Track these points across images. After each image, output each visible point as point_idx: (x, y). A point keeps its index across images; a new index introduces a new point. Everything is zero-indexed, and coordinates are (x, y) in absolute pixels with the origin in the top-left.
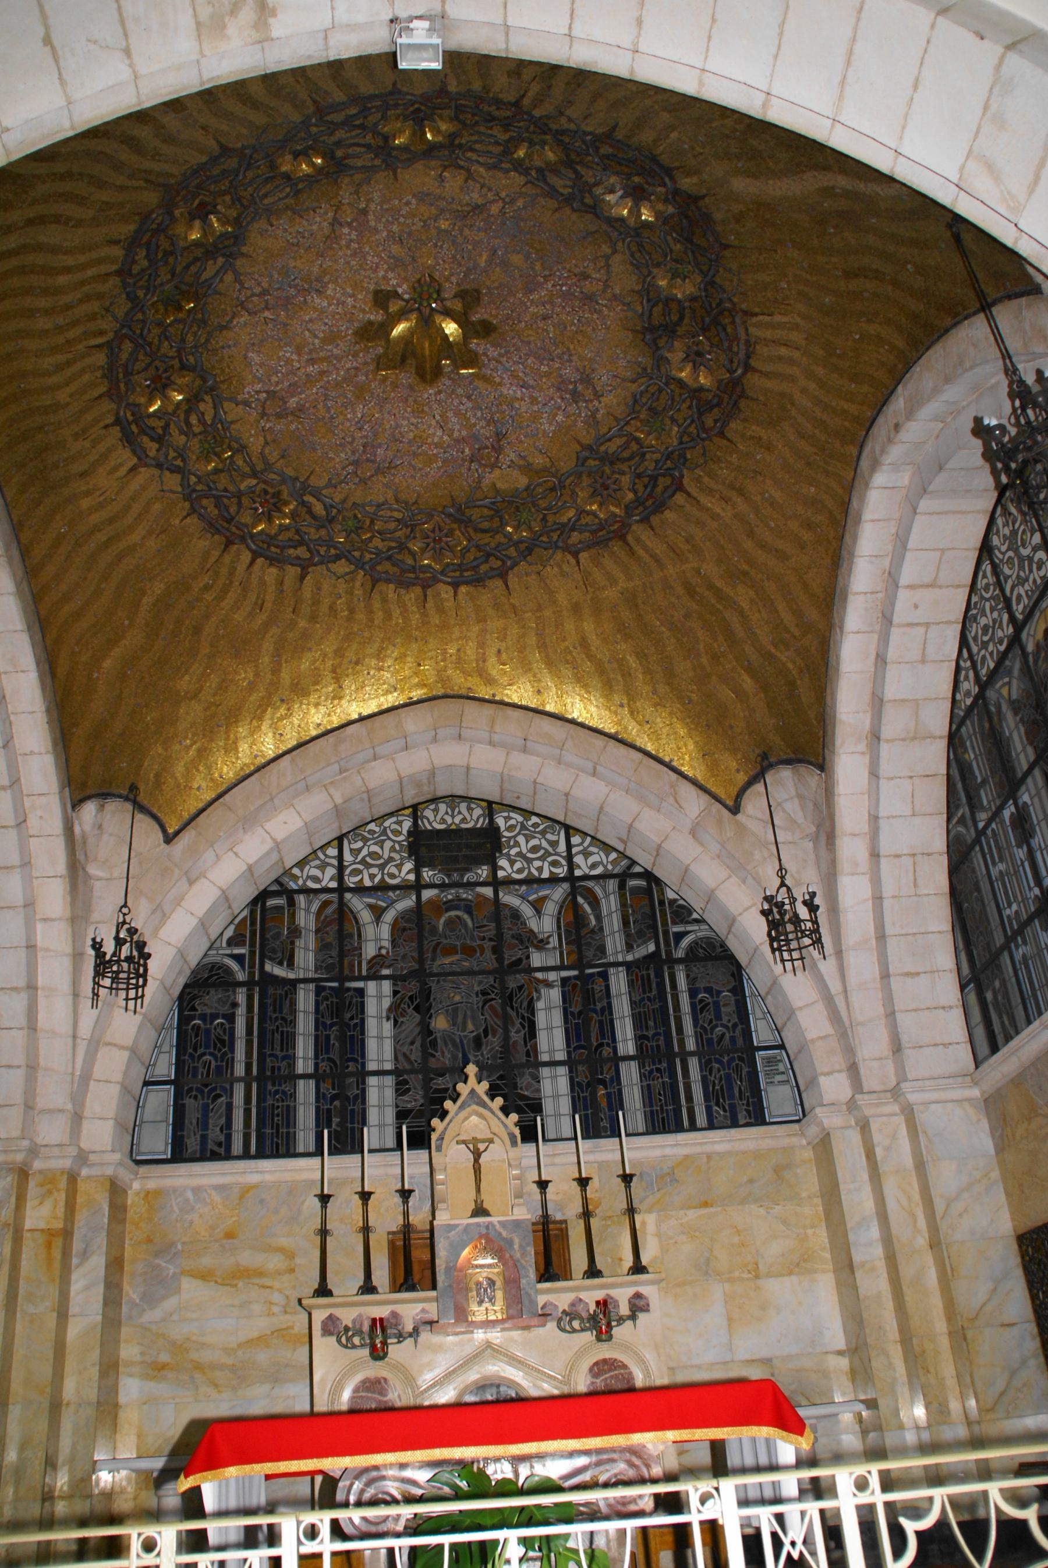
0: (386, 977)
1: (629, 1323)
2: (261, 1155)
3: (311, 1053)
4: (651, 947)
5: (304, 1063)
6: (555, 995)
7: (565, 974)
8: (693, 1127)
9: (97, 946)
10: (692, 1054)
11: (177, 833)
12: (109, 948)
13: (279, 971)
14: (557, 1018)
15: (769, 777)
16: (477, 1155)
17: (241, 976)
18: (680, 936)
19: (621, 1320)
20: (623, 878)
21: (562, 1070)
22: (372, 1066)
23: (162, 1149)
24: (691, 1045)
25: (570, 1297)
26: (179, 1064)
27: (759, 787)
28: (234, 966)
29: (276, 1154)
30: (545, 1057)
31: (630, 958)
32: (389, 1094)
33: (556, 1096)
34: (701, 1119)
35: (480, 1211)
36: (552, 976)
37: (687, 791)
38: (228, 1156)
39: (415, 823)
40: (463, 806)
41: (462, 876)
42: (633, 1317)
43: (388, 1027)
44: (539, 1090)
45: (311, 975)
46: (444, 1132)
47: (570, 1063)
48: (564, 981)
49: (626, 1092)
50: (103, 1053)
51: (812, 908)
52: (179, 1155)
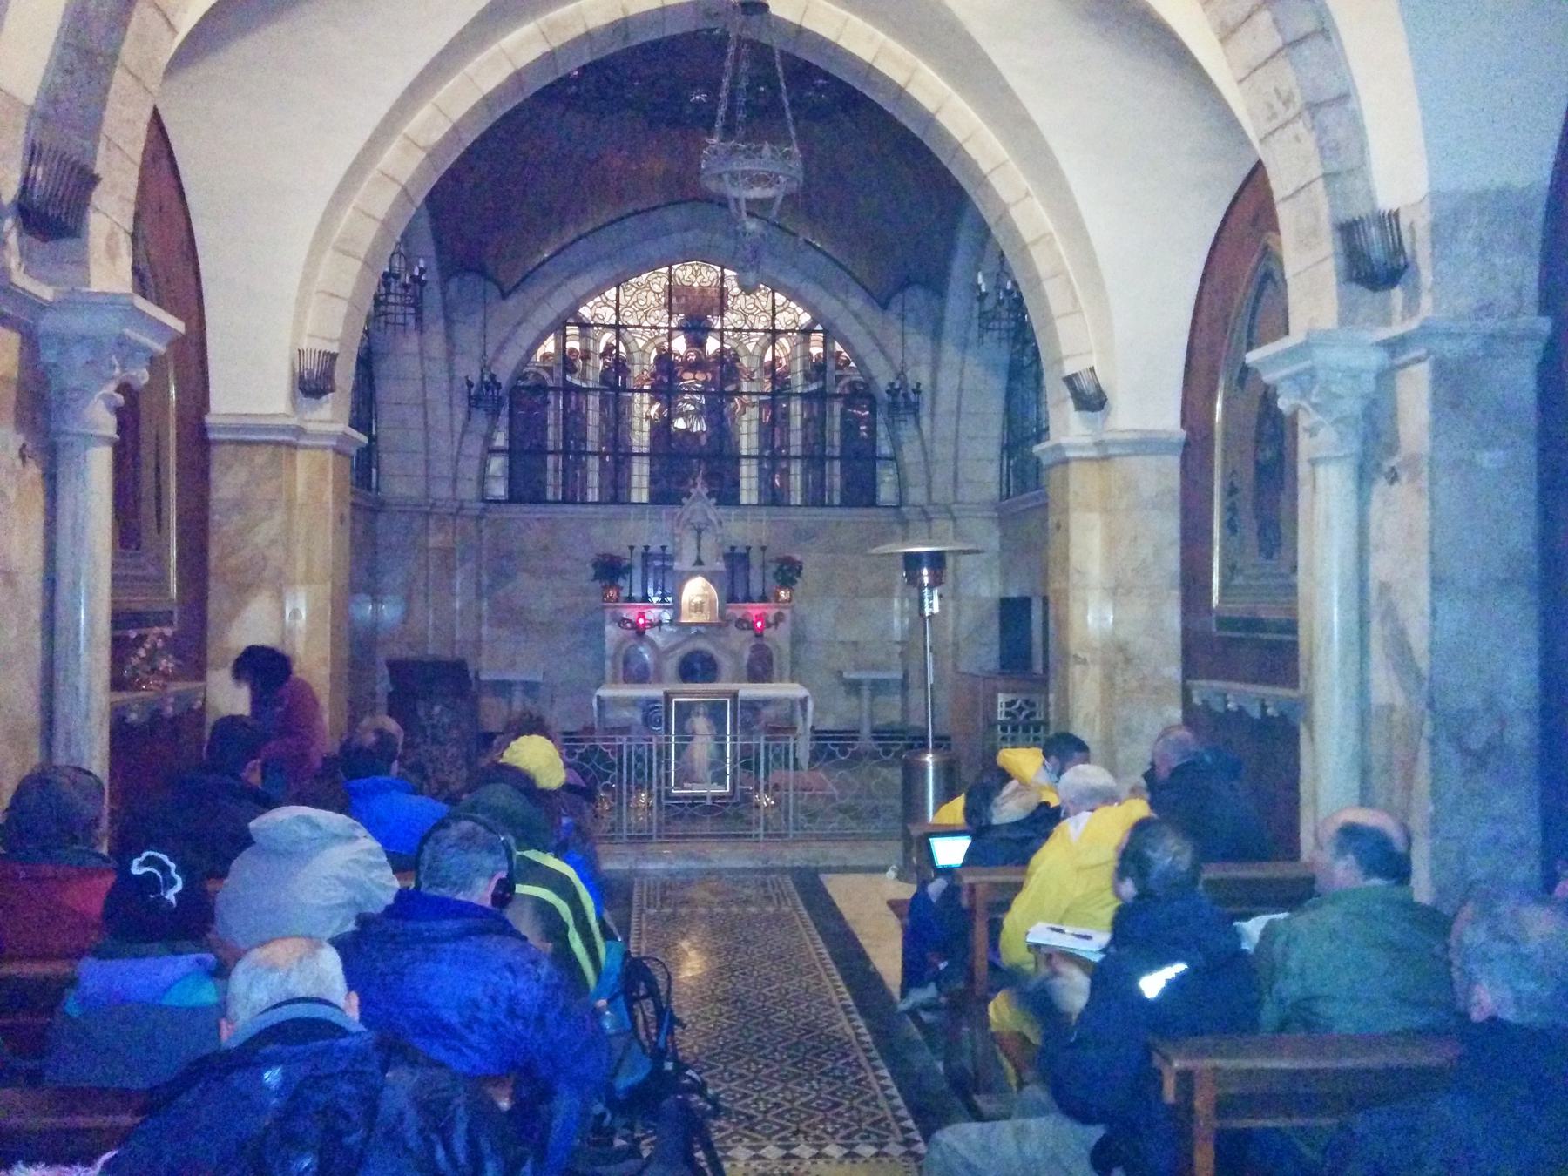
0: (646, 391)
1: (773, 628)
2: (565, 501)
3: (596, 438)
4: (821, 383)
5: (592, 445)
6: (754, 412)
7: (762, 398)
8: (831, 505)
9: (470, 385)
10: (836, 458)
11: (510, 293)
12: (475, 379)
13: (577, 382)
14: (754, 426)
15: (909, 291)
16: (699, 531)
17: (550, 383)
18: (839, 378)
19: (769, 625)
20: (807, 332)
21: (754, 462)
22: (635, 450)
23: (502, 493)
24: (837, 453)
25: (743, 611)
26: (511, 439)
27: (900, 296)
28: (545, 374)
29: (573, 502)
30: (744, 453)
31: (805, 391)
32: (646, 469)
33: (749, 477)
34: (837, 501)
35: (699, 562)
36: (754, 399)
37: (854, 287)
38: (546, 502)
39: (670, 280)
40: (704, 269)
41: (700, 321)
42: (776, 624)
43: (646, 425)
44: (738, 472)
45: (598, 386)
46: (681, 517)
47: (760, 458)
48: (761, 402)
49: (792, 478)
50: (468, 438)
51: (917, 391)
52: (514, 497)
